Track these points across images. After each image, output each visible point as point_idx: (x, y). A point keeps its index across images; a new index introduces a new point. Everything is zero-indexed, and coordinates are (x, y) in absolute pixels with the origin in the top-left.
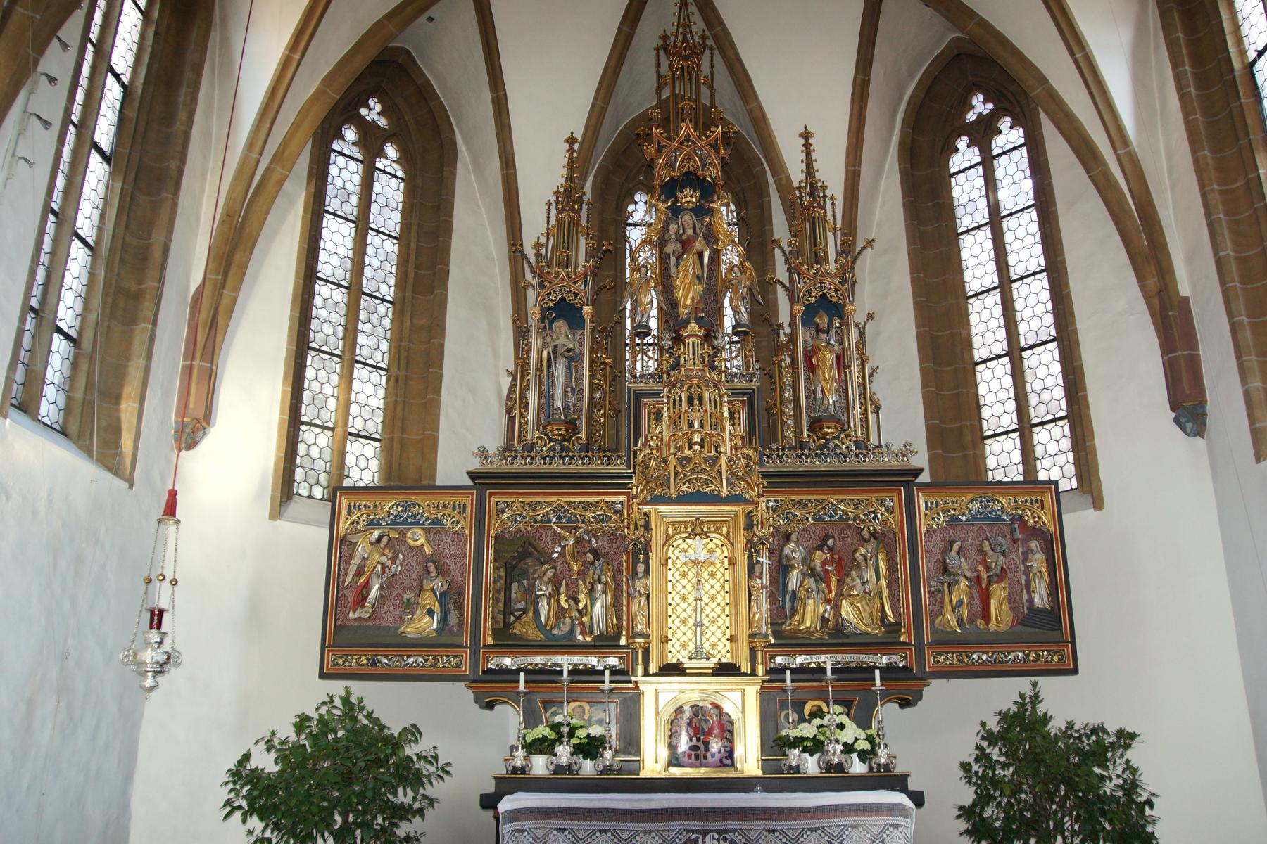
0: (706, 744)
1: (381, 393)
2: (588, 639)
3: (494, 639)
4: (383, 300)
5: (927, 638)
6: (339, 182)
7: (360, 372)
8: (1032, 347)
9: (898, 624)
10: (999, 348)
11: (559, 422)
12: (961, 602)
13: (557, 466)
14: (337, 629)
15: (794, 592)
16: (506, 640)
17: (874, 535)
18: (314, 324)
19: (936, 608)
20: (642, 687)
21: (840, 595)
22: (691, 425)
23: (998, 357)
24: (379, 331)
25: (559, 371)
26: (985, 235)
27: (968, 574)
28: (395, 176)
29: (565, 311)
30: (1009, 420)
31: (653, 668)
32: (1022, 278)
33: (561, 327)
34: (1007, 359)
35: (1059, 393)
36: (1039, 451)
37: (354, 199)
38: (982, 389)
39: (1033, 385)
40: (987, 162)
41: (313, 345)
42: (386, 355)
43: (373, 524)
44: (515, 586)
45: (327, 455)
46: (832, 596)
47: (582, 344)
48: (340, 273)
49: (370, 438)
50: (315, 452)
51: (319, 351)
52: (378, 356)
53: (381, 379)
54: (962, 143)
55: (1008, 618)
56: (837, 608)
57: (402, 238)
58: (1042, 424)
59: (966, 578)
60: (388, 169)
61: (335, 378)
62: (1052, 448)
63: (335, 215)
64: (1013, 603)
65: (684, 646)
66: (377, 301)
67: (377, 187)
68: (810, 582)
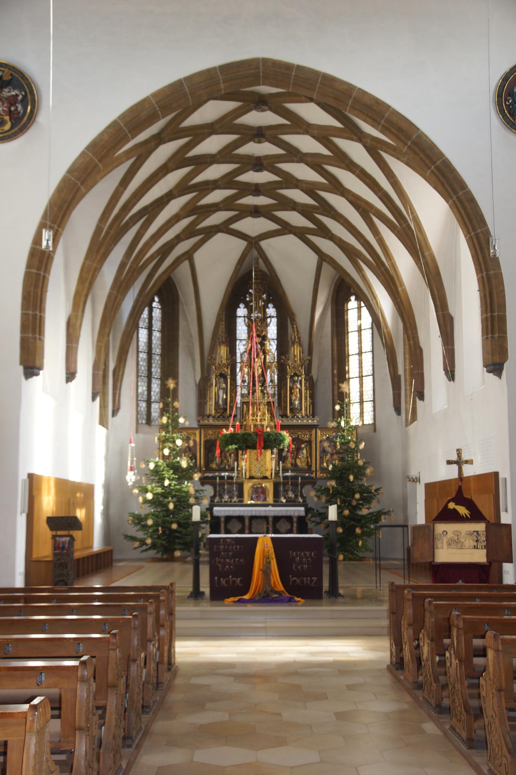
0: (260, 496)
1: (159, 387)
2: (230, 469)
3: (205, 468)
4: (158, 355)
6: (142, 316)
7: (154, 381)
8: (366, 376)
9: (311, 466)
11: (221, 409)
12: (328, 460)
15: (285, 457)
16: (208, 469)
17: (306, 441)
18: (139, 366)
19: (322, 461)
20: (244, 482)
21: (296, 457)
22: (257, 416)
23: (356, 377)
24: (158, 366)
26: (356, 334)
27: (330, 452)
28: (158, 308)
29: (223, 376)
31: (248, 477)
32: (365, 352)
33: (222, 380)
36: (365, 410)
37: (147, 321)
40: (359, 308)
41: (140, 374)
42: (160, 374)
44: (210, 454)
45: (146, 409)
46: (294, 457)
47: (226, 383)
49: (157, 402)
50: (142, 409)
51: (141, 376)
52: (158, 374)
54: (353, 298)
56: (295, 461)
57: (162, 331)
58: (367, 401)
59: (330, 453)
60: (156, 306)
61: (146, 384)
63: (142, 328)
65: (255, 472)
66: (156, 355)
67: (154, 314)
68: (289, 454)
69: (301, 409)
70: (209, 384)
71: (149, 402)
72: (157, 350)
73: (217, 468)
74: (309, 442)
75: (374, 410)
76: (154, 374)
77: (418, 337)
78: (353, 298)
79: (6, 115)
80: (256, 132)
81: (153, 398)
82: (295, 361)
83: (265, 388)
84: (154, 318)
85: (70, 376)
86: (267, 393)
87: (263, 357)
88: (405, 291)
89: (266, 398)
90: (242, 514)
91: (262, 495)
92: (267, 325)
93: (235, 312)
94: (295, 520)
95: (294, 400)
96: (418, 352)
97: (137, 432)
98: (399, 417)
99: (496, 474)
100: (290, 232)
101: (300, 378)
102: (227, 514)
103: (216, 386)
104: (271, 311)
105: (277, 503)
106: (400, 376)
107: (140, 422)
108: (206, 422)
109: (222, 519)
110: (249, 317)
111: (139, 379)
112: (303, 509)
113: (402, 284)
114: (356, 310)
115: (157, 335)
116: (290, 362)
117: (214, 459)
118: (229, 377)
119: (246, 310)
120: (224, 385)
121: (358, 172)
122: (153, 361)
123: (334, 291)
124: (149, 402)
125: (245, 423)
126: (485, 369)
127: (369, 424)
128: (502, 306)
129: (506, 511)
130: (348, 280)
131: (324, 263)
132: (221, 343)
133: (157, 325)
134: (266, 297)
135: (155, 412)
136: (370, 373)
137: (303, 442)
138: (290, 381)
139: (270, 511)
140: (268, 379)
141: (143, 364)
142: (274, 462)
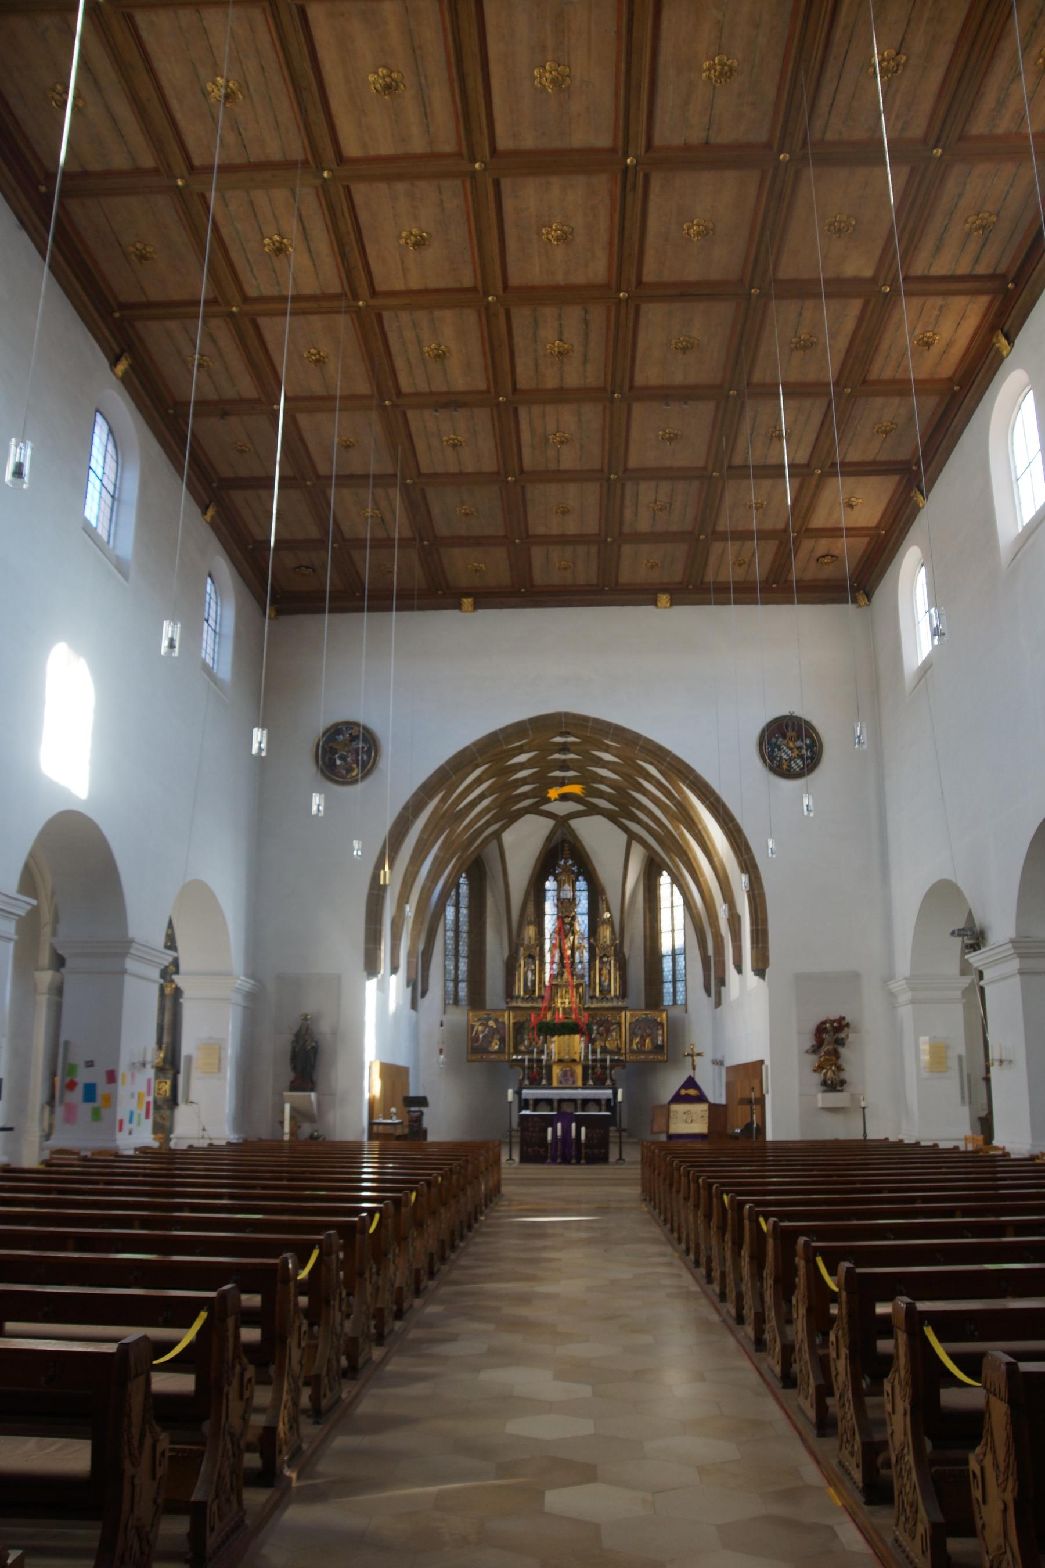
1: (466, 965)
5: (628, 1051)
7: (461, 959)
10: (670, 953)
12: (638, 1043)
13: (529, 1005)
14: (472, 1048)
16: (517, 1052)
18: (447, 946)
21: (606, 1039)
25: (530, 974)
29: (531, 957)
30: (670, 978)
31: (556, 1060)
33: (530, 960)
34: (671, 957)
35: (684, 971)
36: (677, 989)
37: (454, 897)
38: (664, 965)
39: (678, 968)
41: (447, 953)
43: (479, 1020)
44: (519, 1037)
45: (453, 989)
48: (452, 926)
49: (464, 981)
50: (449, 989)
52: (465, 952)
53: (465, 960)
54: (665, 873)
55: (650, 1047)
57: (469, 907)
58: (679, 981)
61: (453, 963)
62: (681, 989)
63: (449, 905)
64: (652, 1042)
67: (461, 891)
68: (598, 1036)
69: (610, 991)
70: (517, 965)
71: (456, 981)
72: (464, 928)
73: (525, 1050)
74: (619, 1024)
75: (686, 991)
76: (461, 952)
77: (719, 925)
78: (665, 873)
79: (354, 763)
80: (561, 747)
81: (460, 977)
82: (605, 942)
83: (575, 969)
84: (461, 895)
85: (394, 970)
86: (576, 975)
87: (572, 938)
88: (706, 881)
89: (575, 980)
90: (550, 1097)
91: (571, 1079)
92: (576, 906)
93: (544, 884)
94: (603, 1103)
95: (605, 981)
96: (720, 939)
97: (445, 1013)
98: (710, 998)
99: (762, 1062)
100: (598, 813)
101: (610, 959)
102: (535, 1097)
103: (525, 966)
104: (581, 884)
105: (585, 1086)
106: (710, 957)
107: (447, 1002)
108: (514, 1004)
109: (531, 1102)
110: (559, 890)
111: (447, 958)
112: (610, 1091)
113: (703, 875)
114: (669, 885)
115: (464, 911)
116: (601, 942)
117: (523, 1041)
118: (537, 958)
119: (555, 883)
120: (533, 967)
121: (654, 782)
122: (460, 939)
123: (646, 865)
124: (456, 981)
125: (553, 1005)
126: (753, 973)
127: (682, 1004)
128: (765, 921)
129: (767, 1092)
130: (657, 859)
131: (633, 842)
132: (529, 923)
133: (464, 901)
134: (577, 869)
135: (462, 992)
136: (682, 952)
137: (613, 1024)
138: (599, 962)
139: (579, 1094)
140: (577, 960)
141: (450, 942)
142: (583, 1045)
